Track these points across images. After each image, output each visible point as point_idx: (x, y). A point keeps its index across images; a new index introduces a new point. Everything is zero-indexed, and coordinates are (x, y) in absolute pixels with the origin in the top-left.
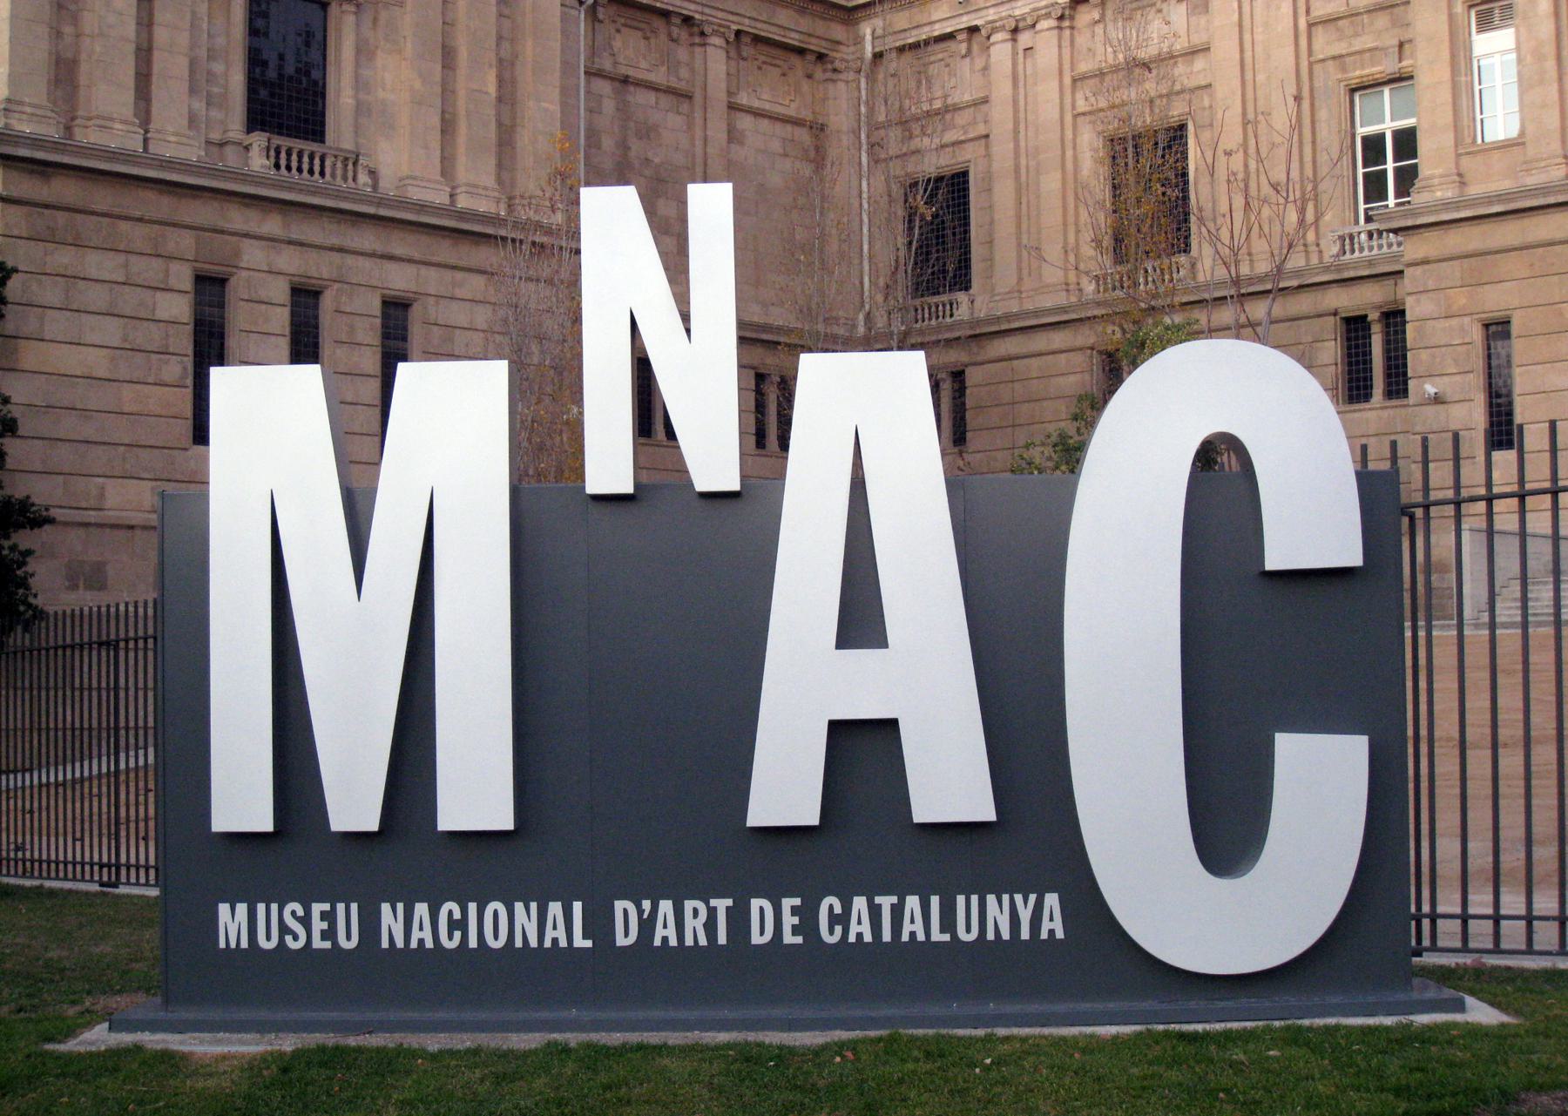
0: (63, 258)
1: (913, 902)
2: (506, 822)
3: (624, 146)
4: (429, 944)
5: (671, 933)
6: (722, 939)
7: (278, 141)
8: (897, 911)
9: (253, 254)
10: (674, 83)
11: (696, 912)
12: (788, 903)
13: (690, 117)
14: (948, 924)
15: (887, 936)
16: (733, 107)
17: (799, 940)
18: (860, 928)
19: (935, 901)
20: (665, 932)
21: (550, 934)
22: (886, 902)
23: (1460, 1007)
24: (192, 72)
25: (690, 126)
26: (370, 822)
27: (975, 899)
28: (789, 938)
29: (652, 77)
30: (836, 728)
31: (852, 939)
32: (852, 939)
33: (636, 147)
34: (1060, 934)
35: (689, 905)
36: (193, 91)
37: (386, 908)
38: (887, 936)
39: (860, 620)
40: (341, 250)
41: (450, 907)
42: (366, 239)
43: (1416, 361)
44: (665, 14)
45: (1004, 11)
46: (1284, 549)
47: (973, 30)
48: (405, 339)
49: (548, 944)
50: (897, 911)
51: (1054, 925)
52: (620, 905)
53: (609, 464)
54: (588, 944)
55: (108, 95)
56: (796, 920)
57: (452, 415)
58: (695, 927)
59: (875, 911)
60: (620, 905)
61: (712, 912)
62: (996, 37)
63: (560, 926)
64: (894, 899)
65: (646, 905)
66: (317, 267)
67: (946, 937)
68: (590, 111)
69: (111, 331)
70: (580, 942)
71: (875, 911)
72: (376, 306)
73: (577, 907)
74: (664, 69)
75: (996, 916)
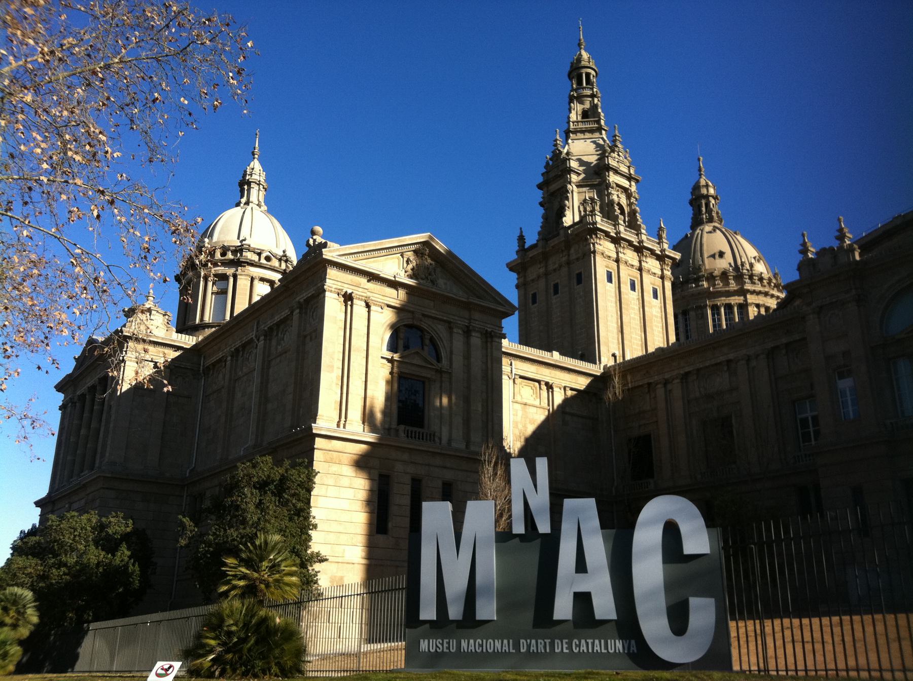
1: (597, 642)
6: (548, 650)
7: (407, 428)
8: (593, 644)
9: (399, 467)
12: (564, 641)
14: (606, 648)
18: (584, 648)
19: (603, 641)
22: (590, 641)
35: (539, 641)
37: (463, 641)
39: (581, 566)
44: (539, 382)
47: (649, 384)
50: (593, 644)
57: (480, 516)
59: (587, 644)
60: (522, 641)
62: (659, 386)
71: (587, 644)
72: (439, 484)
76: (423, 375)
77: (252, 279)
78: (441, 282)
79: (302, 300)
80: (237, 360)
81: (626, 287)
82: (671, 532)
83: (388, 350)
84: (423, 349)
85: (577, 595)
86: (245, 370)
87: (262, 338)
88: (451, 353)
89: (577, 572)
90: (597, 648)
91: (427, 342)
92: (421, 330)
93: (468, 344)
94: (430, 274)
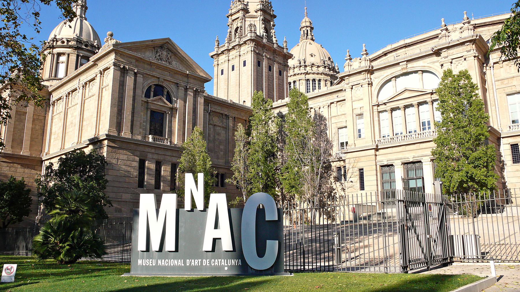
3: (214, 136)
8: (221, 261)
10: (223, 125)
12: (208, 260)
22: (220, 260)
29: (220, 125)
33: (217, 137)
36: (140, 128)
41: (167, 260)
42: (169, 153)
50: (221, 261)
53: (188, 206)
57: (169, 200)
58: (196, 263)
70: (183, 265)
76: (163, 110)
77: (78, 56)
78: (174, 63)
79: (102, 70)
86: (73, 104)
87: (81, 88)
91: (166, 93)
92: (162, 87)
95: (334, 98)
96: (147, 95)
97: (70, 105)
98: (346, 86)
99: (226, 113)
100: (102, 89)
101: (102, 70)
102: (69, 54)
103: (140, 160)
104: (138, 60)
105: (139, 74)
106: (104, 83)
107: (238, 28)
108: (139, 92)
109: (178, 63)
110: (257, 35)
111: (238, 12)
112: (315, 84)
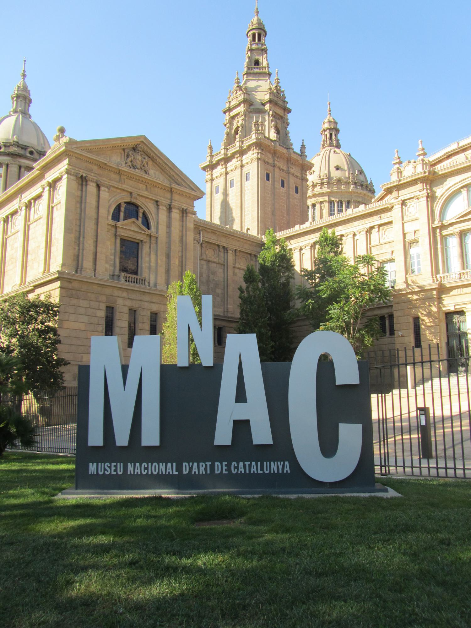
0: (74, 301)
1: (254, 463)
2: (158, 444)
3: (208, 276)
4: (139, 473)
5: (196, 471)
6: (208, 472)
8: (250, 466)
9: (120, 302)
11: (202, 466)
12: (224, 463)
13: (224, 269)
14: (262, 469)
15: (247, 472)
16: (234, 267)
17: (227, 472)
18: (241, 470)
19: (259, 463)
20: (195, 470)
21: (168, 471)
22: (247, 463)
23: (386, 491)
24: (106, 258)
25: (224, 272)
26: (126, 443)
27: (268, 463)
28: (224, 472)
30: (235, 421)
31: (239, 472)
32: (239, 472)
33: (211, 277)
34: (289, 472)
35: (201, 464)
37: (129, 464)
38: (247, 472)
39: (241, 396)
40: (140, 300)
41: (144, 464)
42: (147, 298)
43: (396, 327)
44: (218, 246)
45: (298, 245)
46: (340, 380)
48: (156, 321)
49: (167, 473)
50: (250, 466)
51: (287, 469)
52: (184, 464)
54: (177, 473)
55: (88, 264)
56: (226, 468)
59: (245, 466)
60: (184, 464)
61: (206, 465)
63: (170, 469)
64: (249, 463)
65: (191, 464)
66: (135, 305)
67: (262, 472)
68: (200, 268)
69: (85, 319)
70: (175, 473)
72: (149, 314)
73: (174, 464)
74: (218, 258)
75: (274, 467)
76: (138, 238)
77: (20, 167)
78: (151, 172)
80: (8, 225)
81: (278, 185)
82: (325, 365)
83: (112, 219)
84: (137, 219)
85: (236, 423)
86: (13, 231)
87: (24, 208)
88: (158, 223)
89: (236, 402)
90: (254, 469)
91: (141, 215)
92: (137, 206)
93: (169, 217)
94: (144, 166)
95: (375, 221)
96: (116, 216)
97: (9, 233)
98: (393, 201)
99: (224, 245)
100: (53, 208)
101: (50, 181)
102: (7, 165)
103: (107, 307)
104: (102, 166)
105: (104, 186)
106: (55, 199)
107: (238, 127)
108: (103, 211)
109: (157, 173)
110: (265, 137)
111: (239, 105)
112: (342, 207)
